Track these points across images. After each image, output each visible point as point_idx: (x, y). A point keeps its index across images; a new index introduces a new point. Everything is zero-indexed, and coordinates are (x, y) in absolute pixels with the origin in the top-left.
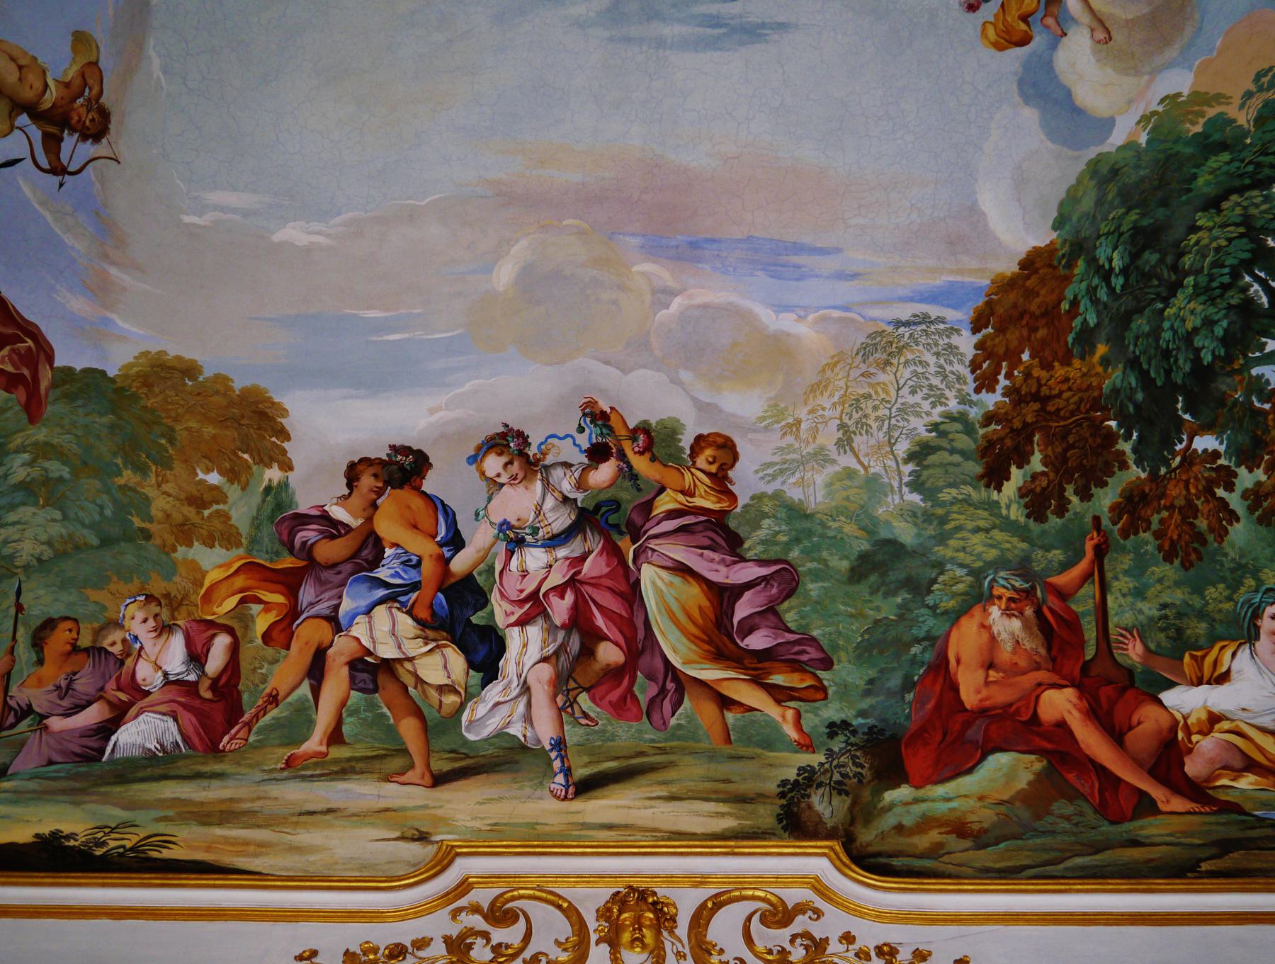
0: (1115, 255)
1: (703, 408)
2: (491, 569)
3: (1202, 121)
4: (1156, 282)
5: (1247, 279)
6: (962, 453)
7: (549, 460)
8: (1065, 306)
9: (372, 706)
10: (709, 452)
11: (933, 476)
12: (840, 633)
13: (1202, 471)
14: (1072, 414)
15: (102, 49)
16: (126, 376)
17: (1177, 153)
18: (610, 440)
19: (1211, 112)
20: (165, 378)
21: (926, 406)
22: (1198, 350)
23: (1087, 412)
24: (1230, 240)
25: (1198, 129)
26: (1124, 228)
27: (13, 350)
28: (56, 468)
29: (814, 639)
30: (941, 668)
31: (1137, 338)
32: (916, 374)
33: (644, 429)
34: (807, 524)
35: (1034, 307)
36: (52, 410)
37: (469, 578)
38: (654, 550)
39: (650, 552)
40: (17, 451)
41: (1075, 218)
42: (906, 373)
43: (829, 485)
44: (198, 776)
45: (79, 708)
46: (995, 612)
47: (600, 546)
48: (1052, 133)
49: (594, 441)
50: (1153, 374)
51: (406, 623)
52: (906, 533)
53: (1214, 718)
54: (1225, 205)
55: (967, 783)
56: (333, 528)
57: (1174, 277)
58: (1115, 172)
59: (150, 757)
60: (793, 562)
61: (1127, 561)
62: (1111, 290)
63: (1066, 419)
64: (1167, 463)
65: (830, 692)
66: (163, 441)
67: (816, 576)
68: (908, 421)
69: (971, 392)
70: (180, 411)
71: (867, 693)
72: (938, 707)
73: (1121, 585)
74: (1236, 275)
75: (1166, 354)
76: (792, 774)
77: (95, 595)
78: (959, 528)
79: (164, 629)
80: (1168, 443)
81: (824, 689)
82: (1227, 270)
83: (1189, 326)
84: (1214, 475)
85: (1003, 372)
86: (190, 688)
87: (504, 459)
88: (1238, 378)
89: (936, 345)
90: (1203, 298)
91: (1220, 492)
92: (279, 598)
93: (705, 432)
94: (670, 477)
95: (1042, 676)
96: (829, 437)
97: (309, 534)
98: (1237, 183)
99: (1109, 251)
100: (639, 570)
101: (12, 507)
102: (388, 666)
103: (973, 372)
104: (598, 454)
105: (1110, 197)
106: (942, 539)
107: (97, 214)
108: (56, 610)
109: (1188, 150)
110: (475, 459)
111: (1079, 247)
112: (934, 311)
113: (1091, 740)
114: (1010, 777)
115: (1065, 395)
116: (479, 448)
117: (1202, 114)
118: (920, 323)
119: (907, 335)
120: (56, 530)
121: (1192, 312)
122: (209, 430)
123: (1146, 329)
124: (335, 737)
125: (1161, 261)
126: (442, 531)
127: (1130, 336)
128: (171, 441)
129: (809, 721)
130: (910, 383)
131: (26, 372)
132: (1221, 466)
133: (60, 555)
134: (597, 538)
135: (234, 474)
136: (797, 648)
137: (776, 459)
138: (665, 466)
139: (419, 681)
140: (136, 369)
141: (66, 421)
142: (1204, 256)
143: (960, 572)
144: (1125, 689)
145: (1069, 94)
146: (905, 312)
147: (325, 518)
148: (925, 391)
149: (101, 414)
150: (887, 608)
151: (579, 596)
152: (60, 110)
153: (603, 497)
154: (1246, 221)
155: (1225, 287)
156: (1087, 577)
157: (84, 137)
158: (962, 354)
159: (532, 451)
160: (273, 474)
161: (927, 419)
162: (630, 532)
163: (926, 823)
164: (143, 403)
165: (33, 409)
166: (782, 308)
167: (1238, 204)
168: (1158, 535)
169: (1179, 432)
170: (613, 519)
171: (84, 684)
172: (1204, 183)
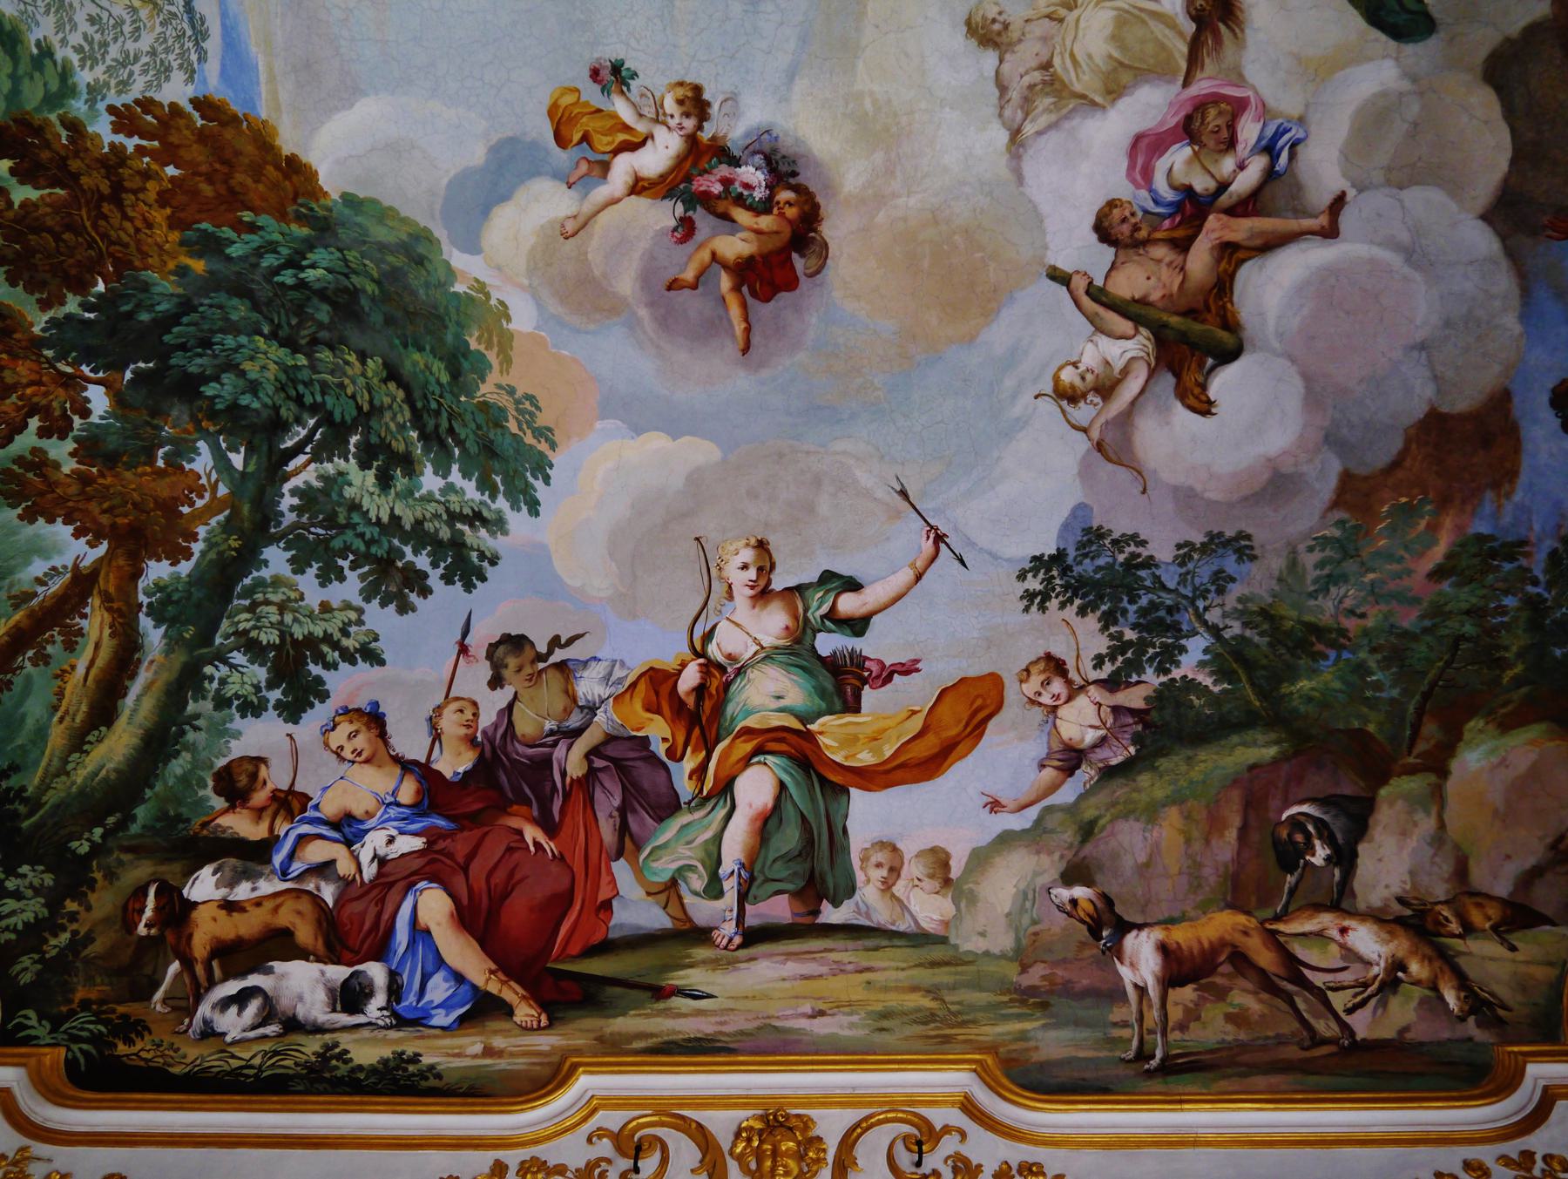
0: (320, 272)
3: (482, 348)
4: (294, 321)
5: (312, 422)
8: (247, 216)
13: (59, 399)
14: (104, 236)
17: (446, 327)
19: (492, 356)
21: (75, 39)
22: (217, 379)
23: (111, 255)
24: (353, 397)
25: (473, 345)
26: (355, 279)
31: (221, 307)
32: (120, 23)
35: (240, 177)
41: (359, 219)
48: (460, 182)
50: (176, 330)
54: (392, 386)
57: (303, 342)
58: (420, 261)
62: (276, 271)
63: (95, 226)
64: (62, 356)
69: (108, 101)
74: (314, 409)
75: (206, 343)
80: (88, 355)
82: (319, 398)
83: (247, 366)
84: (57, 413)
85: (144, 143)
88: (190, 427)
89: (167, 51)
90: (283, 377)
91: (34, 423)
98: (417, 394)
99: (325, 264)
103: (137, 102)
105: (390, 259)
109: (449, 338)
111: (324, 228)
112: (213, 45)
115: (127, 225)
117: (489, 346)
118: (193, 27)
119: (173, 9)
121: (264, 368)
123: (234, 317)
125: (321, 326)
127: (221, 297)
130: (105, 15)
132: (72, 421)
142: (332, 373)
145: (505, 198)
148: (97, 37)
154: (376, 410)
155: (299, 400)
158: (159, 86)
161: (55, 41)
167: (394, 399)
169: (106, 368)
172: (414, 361)
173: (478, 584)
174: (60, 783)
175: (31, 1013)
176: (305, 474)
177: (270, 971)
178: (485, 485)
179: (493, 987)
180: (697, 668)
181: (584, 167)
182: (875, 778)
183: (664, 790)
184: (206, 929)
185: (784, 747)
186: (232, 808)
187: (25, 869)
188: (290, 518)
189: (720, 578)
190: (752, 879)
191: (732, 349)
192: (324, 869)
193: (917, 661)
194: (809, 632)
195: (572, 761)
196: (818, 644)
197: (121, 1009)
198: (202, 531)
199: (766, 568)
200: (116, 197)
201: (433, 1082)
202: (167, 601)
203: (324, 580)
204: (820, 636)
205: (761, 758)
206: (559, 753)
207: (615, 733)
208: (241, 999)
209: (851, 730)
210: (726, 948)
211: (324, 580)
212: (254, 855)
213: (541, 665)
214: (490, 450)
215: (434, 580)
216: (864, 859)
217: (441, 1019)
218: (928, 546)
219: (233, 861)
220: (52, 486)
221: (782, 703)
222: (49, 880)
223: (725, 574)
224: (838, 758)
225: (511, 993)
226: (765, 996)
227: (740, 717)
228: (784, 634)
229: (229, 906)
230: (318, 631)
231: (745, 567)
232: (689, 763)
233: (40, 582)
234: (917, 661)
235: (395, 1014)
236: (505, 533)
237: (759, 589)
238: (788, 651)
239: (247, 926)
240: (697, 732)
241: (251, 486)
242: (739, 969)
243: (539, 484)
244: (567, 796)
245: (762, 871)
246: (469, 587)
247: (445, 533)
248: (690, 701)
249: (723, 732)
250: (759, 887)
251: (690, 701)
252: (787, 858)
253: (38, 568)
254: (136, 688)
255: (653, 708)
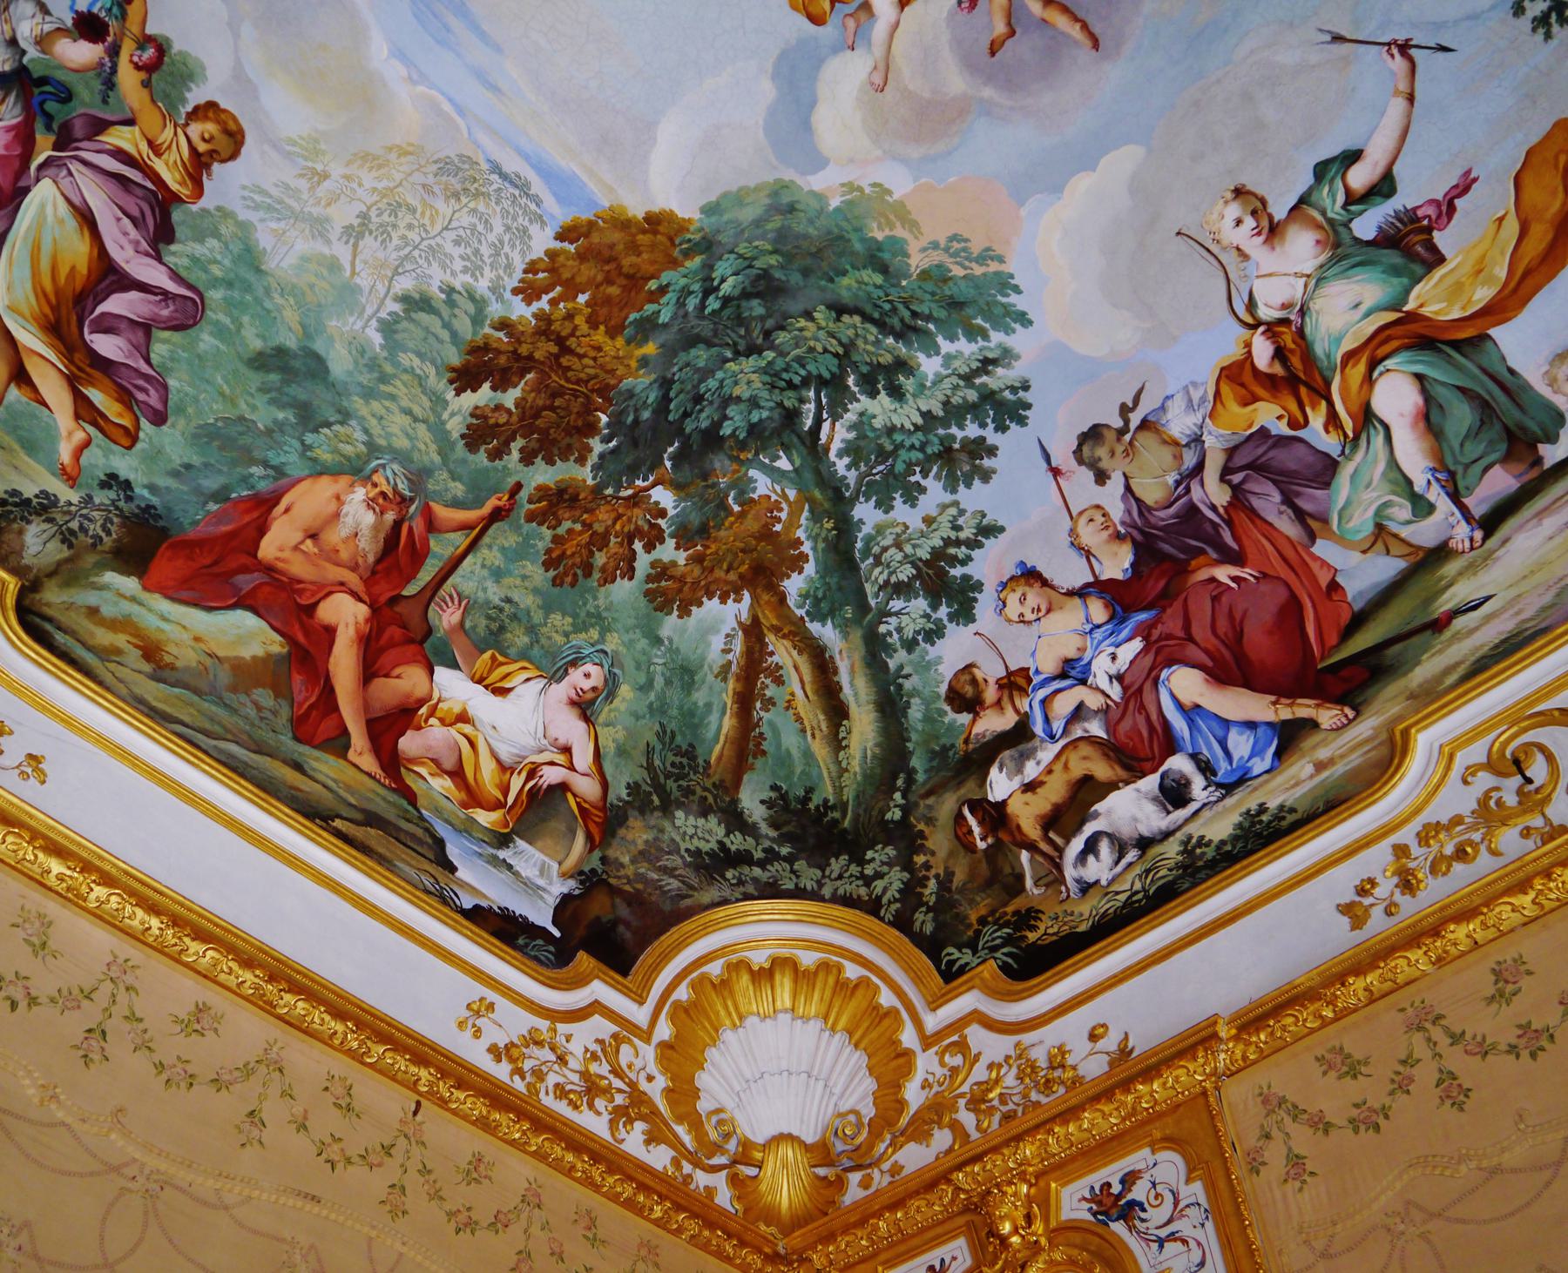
0: (731, 281)
1: (239, 74)
3: (887, 232)
4: (742, 332)
5: (812, 394)
6: (454, 335)
8: (653, 285)
10: (210, 128)
11: (410, 333)
12: (196, 400)
13: (640, 518)
14: (578, 382)
17: (849, 240)
18: (113, 26)
19: (900, 232)
21: (458, 265)
22: (725, 418)
23: (592, 391)
24: (826, 351)
25: (880, 236)
26: (758, 264)
29: (165, 387)
30: (264, 506)
31: (688, 365)
32: (473, 228)
33: (161, 47)
34: (250, 276)
38: (70, 174)
39: (64, 172)
41: (726, 217)
42: (466, 219)
43: (305, 259)
46: (360, 493)
47: (15, 121)
49: (95, 10)
50: (672, 406)
52: (340, 363)
53: (463, 718)
54: (846, 318)
55: (197, 618)
57: (760, 341)
58: (791, 209)
60: (207, 302)
61: (511, 540)
62: (702, 306)
63: (568, 380)
64: (619, 487)
65: (139, 446)
67: (220, 332)
68: (430, 264)
69: (509, 288)
71: (175, 474)
72: (232, 535)
73: (489, 554)
74: (806, 382)
75: (698, 399)
76: (29, 491)
78: (393, 397)
80: (633, 471)
81: (134, 439)
82: (803, 373)
83: (737, 392)
84: (646, 528)
85: (551, 295)
88: (735, 467)
89: (514, 219)
90: (767, 379)
91: (638, 546)
93: (223, 105)
94: (149, 118)
95: (353, 579)
96: (343, 215)
98: (868, 309)
99: (729, 272)
100: (38, 180)
103: (525, 271)
104: (88, 27)
105: (770, 226)
106: (369, 394)
109: (858, 246)
111: (707, 246)
112: (538, 187)
113: (344, 663)
114: (241, 640)
115: (586, 361)
117: (892, 227)
118: (516, 186)
119: (495, 186)
121: (749, 383)
123: (701, 364)
125: (762, 319)
127: (683, 358)
129: (92, 457)
130: (461, 232)
132: (659, 527)
134: (18, 110)
136: (141, 382)
137: (275, 192)
138: (153, 101)
142: (797, 346)
143: (359, 435)
144: (411, 641)
145: (813, 104)
146: (512, 165)
148: (469, 251)
150: (263, 414)
153: (59, 75)
154: (849, 347)
155: (790, 385)
156: (465, 527)
158: (529, 247)
161: (448, 278)
162: (59, 135)
163: (121, 624)
166: (399, 54)
167: (855, 327)
168: (556, 539)
169: (651, 470)
170: (51, 106)
172: (847, 286)
173: (1027, 413)
174: (847, 779)
175: (951, 950)
176: (837, 435)
177: (1096, 815)
178: (973, 333)
179: (1285, 714)
180: (1262, 338)
181: (851, 23)
182: (1502, 308)
183: (1310, 459)
184: (1027, 814)
185: (1395, 344)
186: (976, 715)
187: (869, 854)
188: (852, 477)
189: (1224, 249)
190: (1452, 475)
191: (1085, 53)
192: (1079, 713)
193: (1469, 172)
194: (1341, 229)
195: (1213, 493)
196: (1357, 234)
197: (1010, 909)
198: (800, 534)
199: (1257, 206)
200: (565, 350)
201: (1291, 818)
202: (817, 602)
203: (911, 500)
204: (1353, 225)
205: (1380, 368)
206: (1196, 494)
207: (1231, 444)
208: (1091, 847)
209: (1450, 280)
210: (1472, 549)
211: (911, 500)
212: (1020, 735)
213: (1127, 437)
214: (955, 305)
215: (992, 437)
216: (1552, 382)
217: (1259, 766)
218: (1399, 63)
219: (1007, 754)
220: (681, 580)
221: (1363, 308)
222: (891, 851)
223: (1225, 242)
224: (1456, 314)
225: (1304, 709)
226: (1541, 565)
227: (1333, 350)
228: (1319, 249)
229: (1030, 787)
230: (938, 543)
231: (1239, 222)
232: (1317, 419)
233: (726, 651)
234: (1469, 172)
235: (1219, 785)
236: (1018, 357)
237: (1266, 231)
238: (1335, 260)
239: (1055, 791)
240: (1303, 391)
241: (808, 476)
242: (1498, 559)
243: (1013, 298)
244: (1230, 523)
245: (1456, 462)
246: (1022, 421)
247: (972, 396)
248: (1278, 369)
249: (1327, 373)
250: (1464, 477)
251: (1278, 369)
252: (1473, 434)
253: (717, 643)
254: (844, 678)
255: (1249, 400)
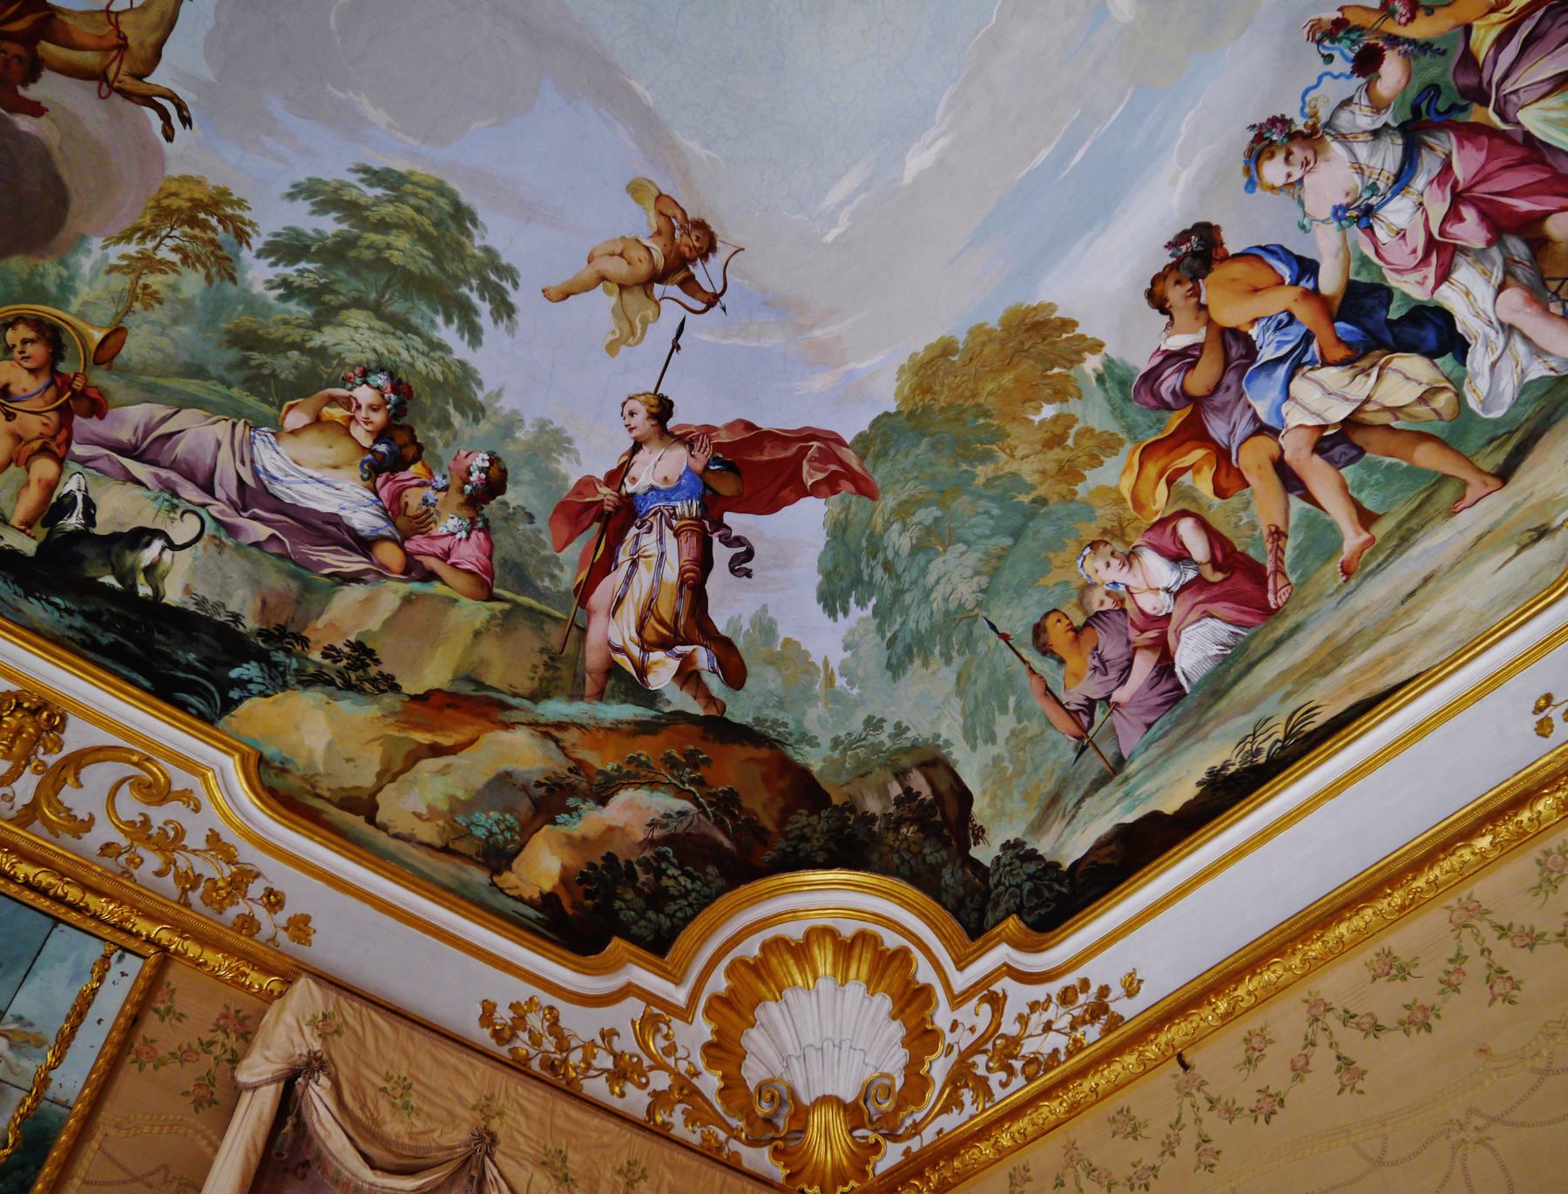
2: (1365, 261)
7: (1324, 116)
9: (1372, 467)
15: (653, 179)
16: (905, 400)
18: (1368, 39)
20: (934, 373)
27: (809, 461)
28: (926, 515)
36: (878, 477)
37: (1351, 288)
38: (1515, 92)
39: (1513, 98)
40: (886, 530)
44: (1278, 643)
45: (1127, 669)
47: (1453, 139)
49: (1352, 55)
51: (1331, 376)
56: (1185, 358)
59: (1224, 661)
66: (981, 421)
70: (970, 386)
77: (1050, 580)
79: (1130, 558)
86: (1199, 583)
87: (1280, 157)
92: (1198, 454)
97: (1170, 381)
100: (1518, 123)
101: (924, 572)
102: (1351, 423)
104: (1367, 63)
107: (767, 303)
108: (1034, 616)
110: (1251, 185)
116: (1247, 171)
120: (972, 558)
122: (1007, 379)
124: (1366, 519)
126: (1285, 271)
128: (987, 414)
131: (833, 467)
133: (994, 574)
134: (1443, 136)
135: (1060, 394)
139: (1395, 410)
140: (906, 389)
141: (897, 475)
147: (1170, 356)
149: (917, 446)
151: (1476, 203)
152: (672, 255)
153: (1412, 94)
157: (705, 257)
159: (1300, 124)
160: (1092, 363)
162: (1473, 100)
164: (937, 408)
165: (865, 488)
170: (1442, 105)
171: (1112, 649)
